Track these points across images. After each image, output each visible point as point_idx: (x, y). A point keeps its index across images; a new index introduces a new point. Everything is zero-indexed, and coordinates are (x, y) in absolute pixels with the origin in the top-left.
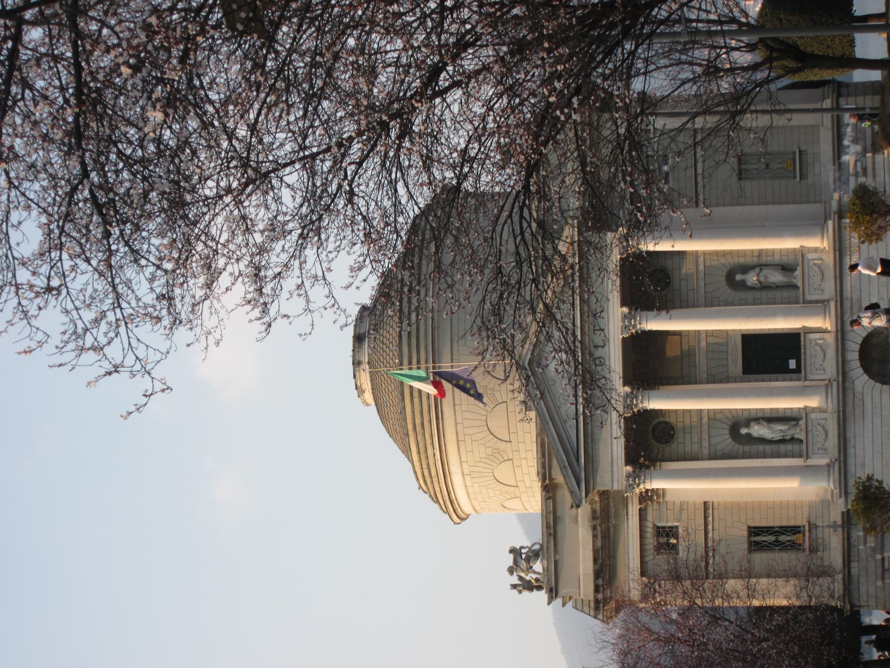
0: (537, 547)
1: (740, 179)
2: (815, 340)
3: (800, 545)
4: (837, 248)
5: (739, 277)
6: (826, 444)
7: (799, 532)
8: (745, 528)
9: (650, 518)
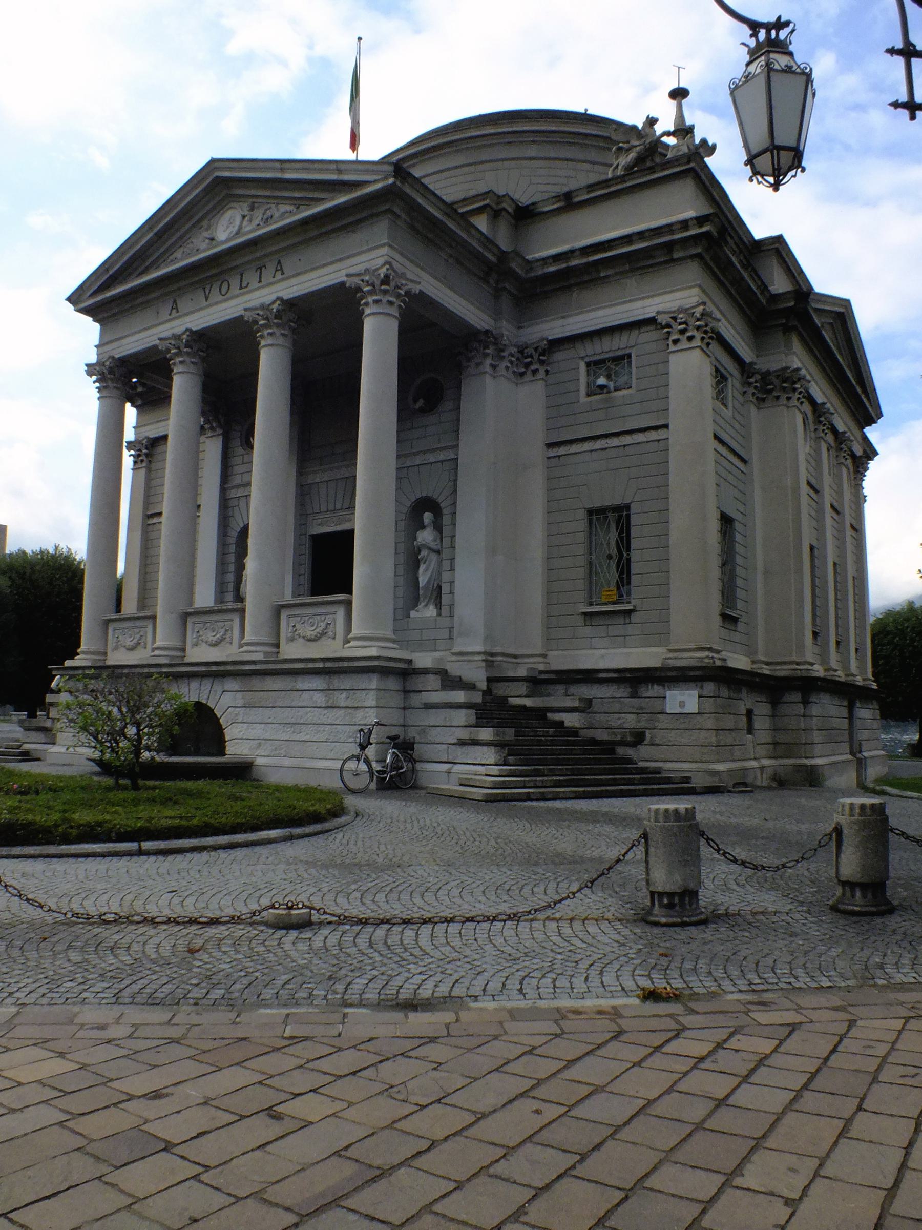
1: (590, 512)
2: (232, 628)
4: (328, 665)
5: (427, 517)
6: (123, 649)
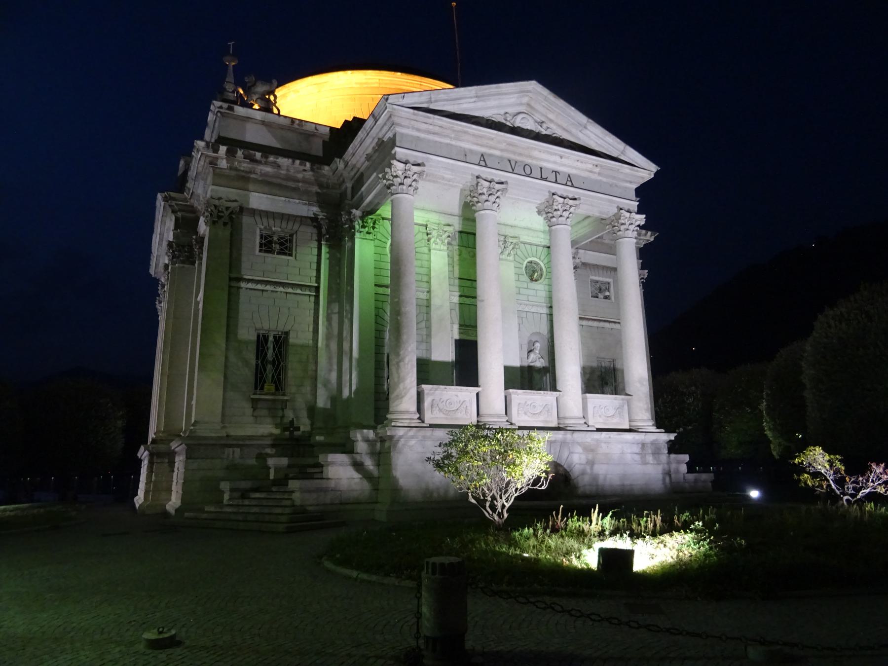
0: (275, 111)
3: (262, 388)
7: (277, 389)
8: (286, 330)
9: (303, 228)
